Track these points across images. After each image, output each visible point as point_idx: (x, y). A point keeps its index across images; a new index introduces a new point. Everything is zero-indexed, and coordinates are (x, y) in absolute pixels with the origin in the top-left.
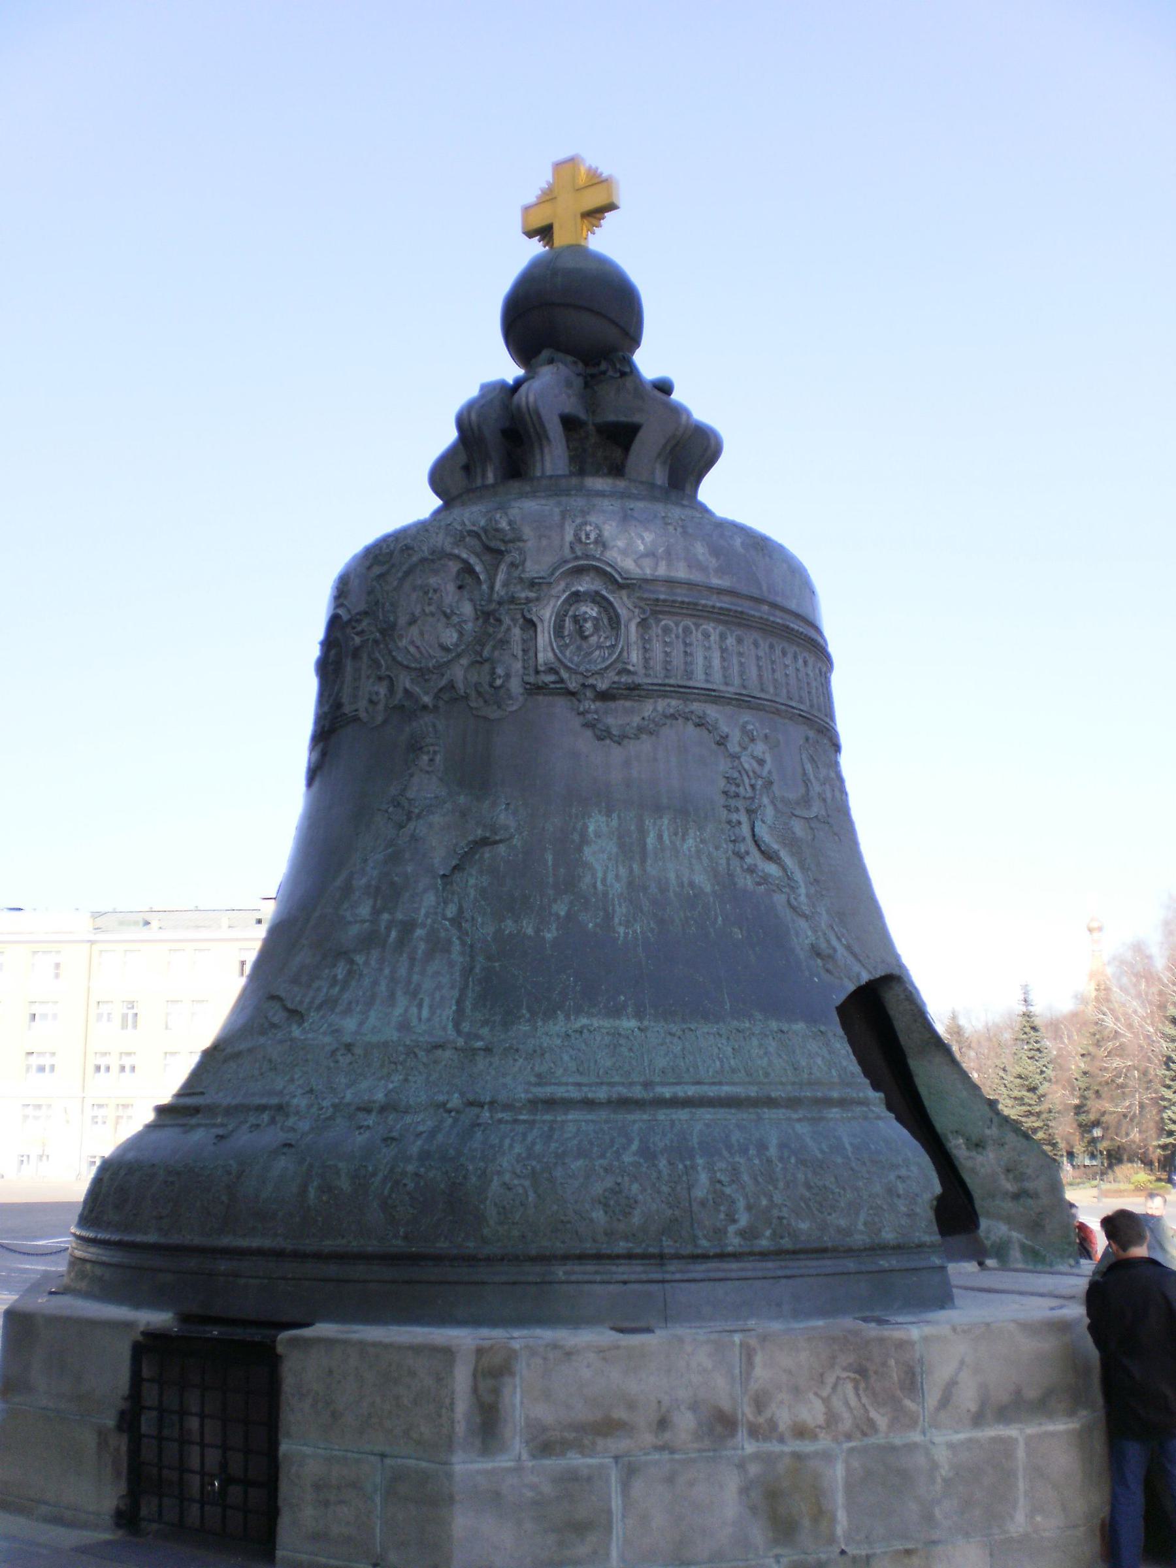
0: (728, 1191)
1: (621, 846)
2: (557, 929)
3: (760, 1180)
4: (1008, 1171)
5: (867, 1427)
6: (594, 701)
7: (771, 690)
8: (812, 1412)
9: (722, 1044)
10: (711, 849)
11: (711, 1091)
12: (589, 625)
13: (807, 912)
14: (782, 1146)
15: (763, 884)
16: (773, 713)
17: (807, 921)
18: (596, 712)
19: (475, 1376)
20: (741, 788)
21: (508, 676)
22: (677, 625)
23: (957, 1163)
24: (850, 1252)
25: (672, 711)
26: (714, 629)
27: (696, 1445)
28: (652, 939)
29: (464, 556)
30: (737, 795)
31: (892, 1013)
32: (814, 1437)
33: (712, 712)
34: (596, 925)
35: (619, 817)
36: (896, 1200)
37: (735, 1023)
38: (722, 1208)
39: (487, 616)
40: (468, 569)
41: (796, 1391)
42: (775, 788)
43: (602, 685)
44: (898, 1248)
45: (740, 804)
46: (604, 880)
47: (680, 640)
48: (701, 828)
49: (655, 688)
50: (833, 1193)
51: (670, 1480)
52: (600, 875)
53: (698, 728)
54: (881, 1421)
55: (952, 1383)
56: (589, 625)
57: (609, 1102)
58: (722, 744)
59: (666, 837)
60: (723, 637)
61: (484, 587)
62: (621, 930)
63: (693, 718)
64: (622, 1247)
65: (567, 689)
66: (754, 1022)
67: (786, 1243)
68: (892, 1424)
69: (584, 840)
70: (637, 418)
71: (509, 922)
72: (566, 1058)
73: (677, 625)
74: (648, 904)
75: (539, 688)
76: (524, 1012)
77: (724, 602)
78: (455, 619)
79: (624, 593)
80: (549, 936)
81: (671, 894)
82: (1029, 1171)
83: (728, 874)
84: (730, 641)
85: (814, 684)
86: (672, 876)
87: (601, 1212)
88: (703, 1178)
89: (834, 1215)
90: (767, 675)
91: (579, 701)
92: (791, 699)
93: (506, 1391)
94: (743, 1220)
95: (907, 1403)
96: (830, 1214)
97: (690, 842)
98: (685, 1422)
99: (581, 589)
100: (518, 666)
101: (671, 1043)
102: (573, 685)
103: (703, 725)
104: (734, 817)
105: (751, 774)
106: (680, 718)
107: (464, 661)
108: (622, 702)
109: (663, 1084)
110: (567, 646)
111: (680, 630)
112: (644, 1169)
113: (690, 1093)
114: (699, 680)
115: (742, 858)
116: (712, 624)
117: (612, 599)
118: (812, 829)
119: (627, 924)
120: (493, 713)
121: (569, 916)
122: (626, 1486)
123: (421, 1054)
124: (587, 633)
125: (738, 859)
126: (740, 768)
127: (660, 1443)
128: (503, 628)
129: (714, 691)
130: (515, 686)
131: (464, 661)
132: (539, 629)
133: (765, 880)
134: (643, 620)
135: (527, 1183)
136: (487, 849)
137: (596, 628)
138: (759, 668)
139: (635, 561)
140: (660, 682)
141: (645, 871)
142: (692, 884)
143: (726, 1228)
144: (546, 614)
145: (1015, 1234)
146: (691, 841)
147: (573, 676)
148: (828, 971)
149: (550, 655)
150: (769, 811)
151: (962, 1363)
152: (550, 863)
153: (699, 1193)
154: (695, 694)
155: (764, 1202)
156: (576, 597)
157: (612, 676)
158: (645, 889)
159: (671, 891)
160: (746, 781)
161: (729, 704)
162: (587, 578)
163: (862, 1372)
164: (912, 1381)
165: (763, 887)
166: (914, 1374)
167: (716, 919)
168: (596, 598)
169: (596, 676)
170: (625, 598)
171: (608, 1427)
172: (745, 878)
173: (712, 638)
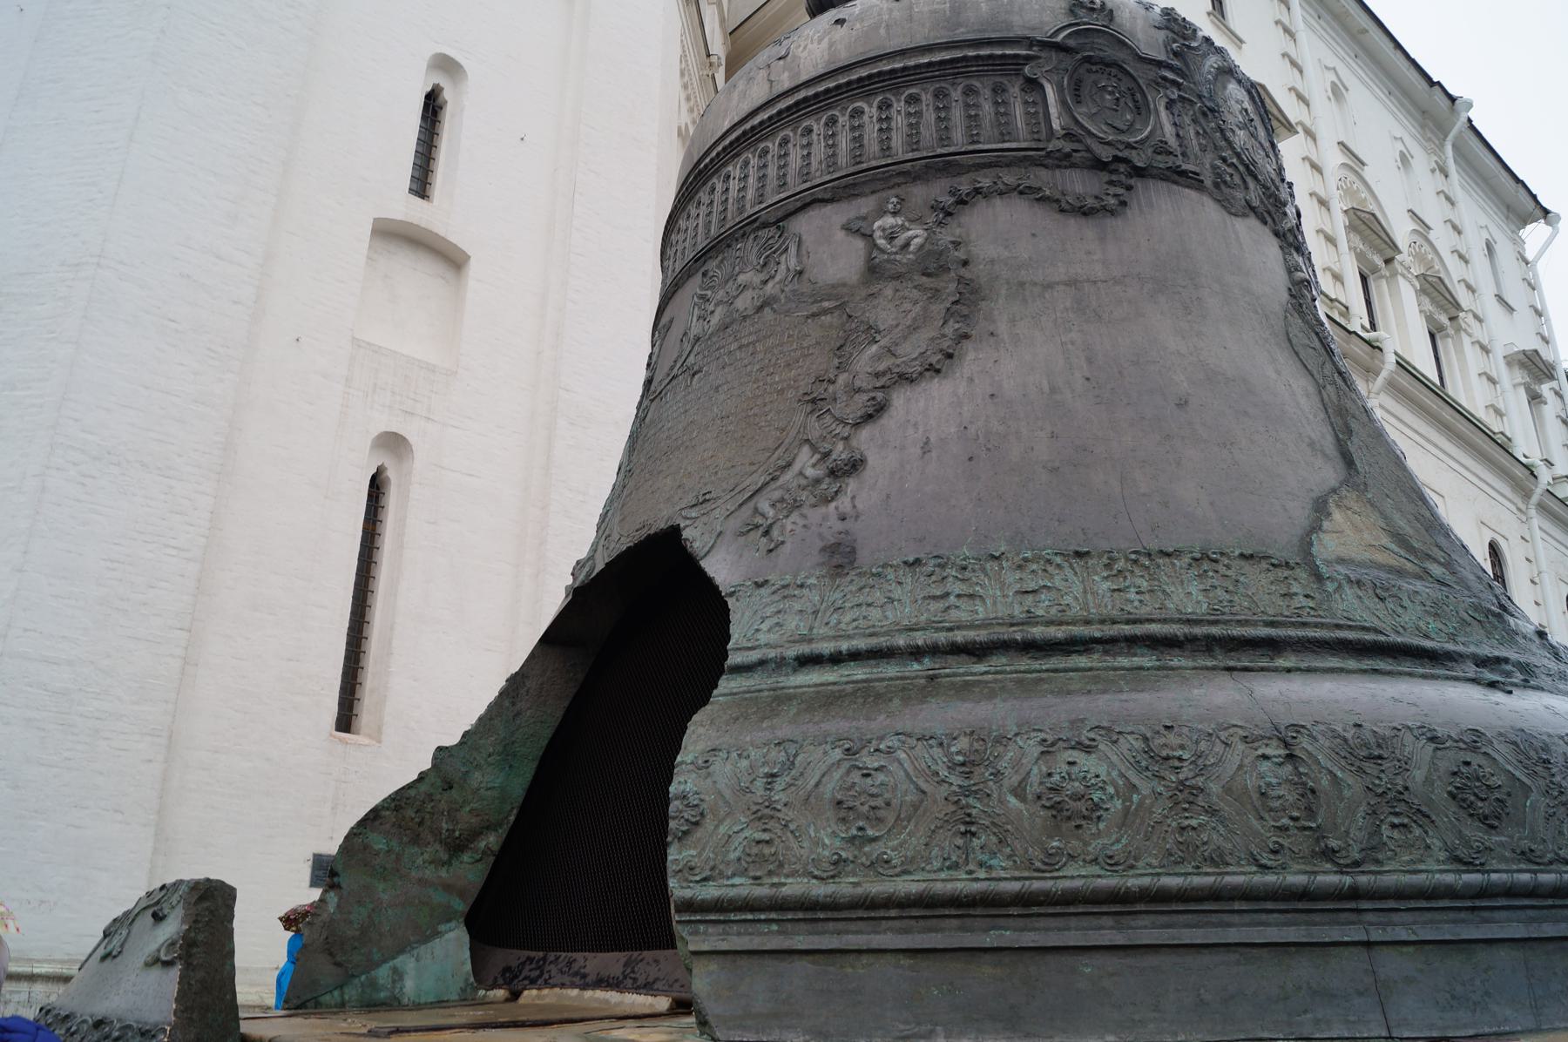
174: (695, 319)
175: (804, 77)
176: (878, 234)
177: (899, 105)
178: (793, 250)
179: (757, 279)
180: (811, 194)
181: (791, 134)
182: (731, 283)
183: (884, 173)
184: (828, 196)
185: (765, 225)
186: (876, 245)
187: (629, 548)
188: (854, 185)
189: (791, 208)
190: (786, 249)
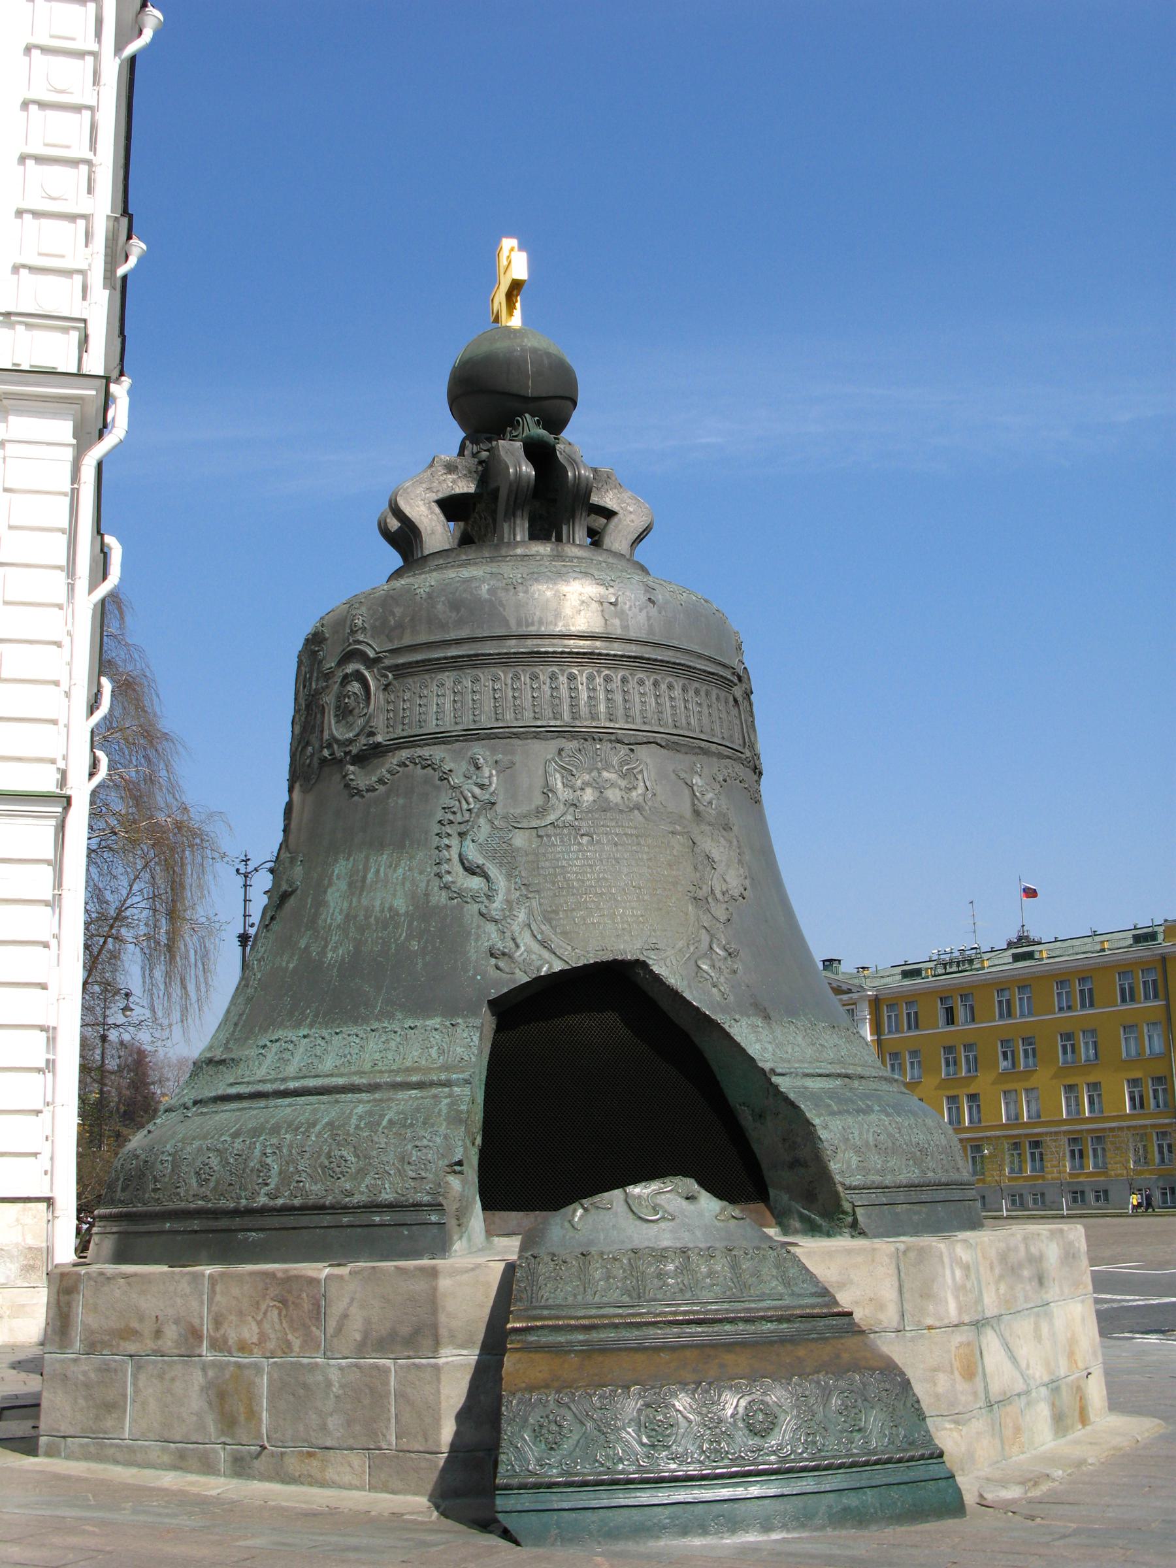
0: (269, 1161)
1: (351, 885)
3: (294, 1151)
4: (784, 1140)
5: (287, 1348)
8: (250, 1332)
11: (311, 1083)
13: (497, 917)
14: (331, 1124)
19: (58, 1293)
20: (459, 815)
24: (345, 1209)
27: (176, 1351)
32: (251, 1352)
33: (437, 753)
34: (318, 953)
36: (407, 1167)
37: (375, 1025)
39: (308, 706)
41: (241, 1314)
42: (498, 808)
43: (354, 751)
44: (390, 1206)
46: (333, 914)
48: (412, 858)
50: (346, 1161)
51: (161, 1377)
54: (296, 1344)
55: (345, 1316)
58: (445, 779)
59: (382, 869)
60: (457, 682)
62: (330, 955)
67: (297, 1202)
68: (301, 1347)
69: (330, 884)
80: (291, 966)
81: (372, 920)
82: (799, 1140)
83: (425, 895)
85: (584, 695)
86: (377, 903)
88: (257, 1152)
93: (74, 1304)
94: (273, 1182)
95: (314, 1329)
96: (339, 1178)
97: (400, 871)
98: (171, 1332)
102: (339, 754)
103: (429, 765)
104: (446, 841)
105: (471, 800)
114: (431, 727)
115: (441, 878)
116: (447, 674)
117: (366, 673)
118: (539, 836)
119: (334, 952)
121: (307, 947)
122: (135, 1377)
127: (156, 1348)
135: (170, 1158)
139: (387, 636)
141: (359, 902)
142: (391, 909)
143: (260, 1189)
145: (793, 1203)
148: (498, 968)
150: (483, 830)
151: (352, 1299)
155: (291, 1169)
156: (346, 679)
157: (363, 740)
158: (355, 917)
160: (465, 806)
163: (284, 1302)
164: (318, 1312)
166: (319, 1306)
167: (400, 936)
171: (129, 1333)
175: (632, 635)
176: (695, 788)
177: (691, 693)
178: (645, 773)
179: (623, 783)
182: (595, 774)
184: (663, 744)
185: (619, 741)
187: (596, 963)
189: (640, 740)
190: (641, 771)
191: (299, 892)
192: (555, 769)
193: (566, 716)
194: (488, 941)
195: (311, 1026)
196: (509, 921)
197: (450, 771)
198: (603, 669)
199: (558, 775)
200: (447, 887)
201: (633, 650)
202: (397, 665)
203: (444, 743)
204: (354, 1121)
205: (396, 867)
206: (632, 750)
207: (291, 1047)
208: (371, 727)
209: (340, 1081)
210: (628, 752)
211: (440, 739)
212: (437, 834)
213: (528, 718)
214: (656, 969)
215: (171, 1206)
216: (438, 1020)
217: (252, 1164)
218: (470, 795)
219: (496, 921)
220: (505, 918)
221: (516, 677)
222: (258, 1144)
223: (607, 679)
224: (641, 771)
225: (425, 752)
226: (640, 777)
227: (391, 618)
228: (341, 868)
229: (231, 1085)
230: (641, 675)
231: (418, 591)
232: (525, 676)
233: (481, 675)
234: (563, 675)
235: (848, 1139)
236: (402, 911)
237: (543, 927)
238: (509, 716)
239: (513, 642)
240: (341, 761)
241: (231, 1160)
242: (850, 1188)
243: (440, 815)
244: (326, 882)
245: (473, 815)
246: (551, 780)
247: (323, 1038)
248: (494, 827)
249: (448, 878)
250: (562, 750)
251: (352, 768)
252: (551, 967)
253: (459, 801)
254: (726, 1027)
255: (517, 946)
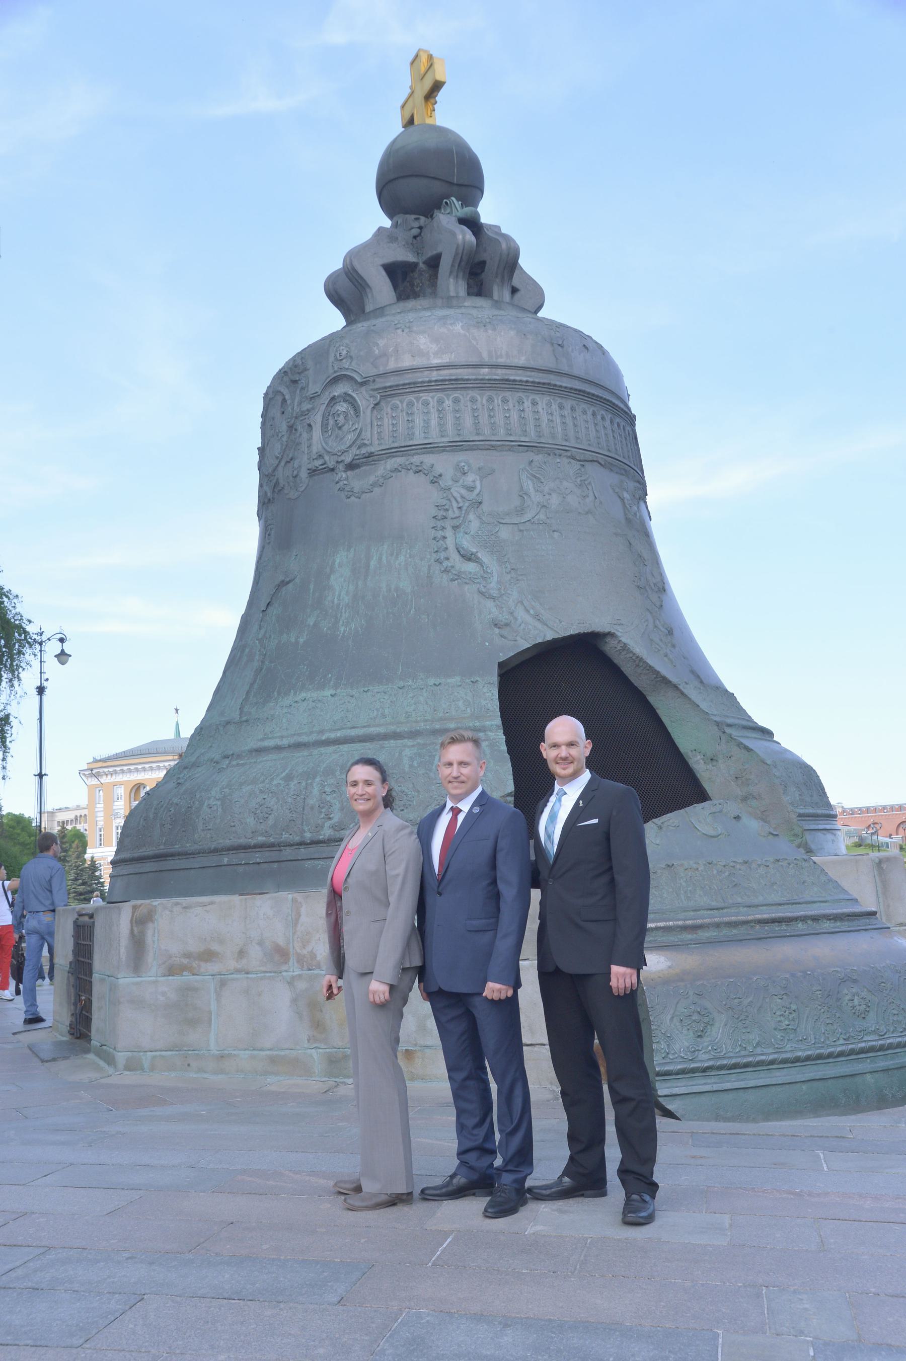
0: (328, 798)
2: (307, 635)
6: (345, 471)
7: (487, 431)
9: (384, 698)
10: (417, 561)
11: (353, 733)
12: (341, 419)
13: (495, 595)
15: (457, 579)
16: (490, 449)
17: (494, 601)
18: (347, 479)
20: (450, 512)
21: (300, 467)
22: (402, 402)
23: (698, 776)
25: (396, 466)
26: (433, 398)
28: (360, 632)
29: (282, 390)
30: (445, 518)
31: (616, 661)
33: (428, 459)
35: (355, 550)
37: (401, 684)
38: (323, 810)
39: (291, 428)
40: (284, 400)
42: (485, 507)
43: (348, 459)
45: (448, 524)
46: (339, 595)
47: (404, 413)
49: (384, 452)
50: (407, 795)
52: (337, 593)
53: (417, 474)
56: (341, 419)
57: (289, 746)
58: (436, 482)
59: (384, 558)
60: (440, 402)
61: (290, 409)
62: (342, 629)
63: (413, 467)
64: (261, 839)
65: (328, 467)
66: (416, 680)
69: (332, 571)
70: (439, 250)
71: (285, 635)
72: (284, 720)
73: (402, 402)
74: (363, 608)
75: (315, 471)
76: (275, 693)
77: (445, 374)
78: (280, 435)
79: (363, 389)
80: (301, 640)
83: (428, 577)
84: (448, 403)
85: (545, 418)
87: (253, 818)
88: (316, 791)
89: (405, 811)
90: (484, 420)
91: (337, 474)
92: (511, 435)
94: (337, 817)
96: (403, 810)
99: (336, 394)
100: (305, 458)
101: (349, 702)
102: (331, 464)
103: (420, 471)
104: (441, 533)
105: (459, 499)
106: (403, 470)
107: (283, 464)
108: (364, 468)
109: (331, 730)
110: (330, 436)
111: (405, 405)
112: (282, 787)
113: (338, 735)
114: (419, 439)
116: (431, 394)
117: (354, 395)
118: (521, 531)
120: (293, 494)
123: (221, 728)
124: (340, 425)
125: (439, 564)
126: (450, 497)
128: (298, 434)
129: (430, 444)
130: (304, 474)
131: (283, 464)
132: (314, 429)
133: (459, 576)
134: (376, 404)
135: (219, 803)
136: (284, 588)
137: (345, 418)
138: (476, 417)
140: (388, 447)
143: (324, 823)
144: (317, 419)
146: (402, 557)
147: (332, 457)
149: (320, 446)
152: (312, 591)
153: (311, 802)
154: (413, 450)
157: (354, 451)
159: (381, 597)
160: (455, 505)
161: (444, 451)
162: (341, 385)
165: (456, 582)
167: (410, 611)
168: (347, 398)
169: (345, 454)
170: (364, 392)
172: (442, 578)
173: (431, 405)
174: (531, 487)
175: (576, 372)
176: (626, 501)
177: (616, 425)
180: (597, 457)
181: (577, 408)
183: (621, 465)
184: (603, 463)
185: (573, 458)
186: (626, 507)
188: (612, 464)
190: (590, 483)
191: (297, 580)
192: (527, 477)
193: (533, 434)
194: (490, 614)
195: (336, 687)
196: (505, 598)
197: (440, 475)
198: (557, 398)
199: (529, 482)
200: (446, 571)
201: (577, 385)
202: (385, 388)
203: (432, 453)
204: (406, 761)
205: (397, 555)
206: (583, 466)
207: (319, 705)
208: (363, 439)
209: (382, 730)
210: (579, 467)
211: (428, 448)
212: (433, 528)
213: (501, 434)
214: (624, 640)
215: (228, 843)
216: (458, 678)
217: (311, 802)
218: (459, 495)
219: (494, 598)
220: (501, 596)
221: (490, 399)
222: (315, 785)
223: (561, 407)
224: (590, 483)
225: (416, 459)
226: (590, 488)
227: (375, 348)
228: (342, 557)
229: (262, 740)
230: (584, 406)
231: (399, 326)
232: (498, 400)
233: (461, 397)
234: (528, 400)
235: (790, 777)
236: (409, 590)
237: (533, 603)
238: (487, 431)
239: (486, 370)
240: (333, 470)
241: (290, 800)
242: (800, 815)
243: (434, 511)
244: (328, 570)
245: (463, 512)
246: (525, 487)
247: (352, 696)
248: (482, 522)
249: (450, 565)
250: (532, 461)
251: (344, 475)
252: (545, 636)
253: (449, 500)
254: (681, 687)
255: (516, 619)
